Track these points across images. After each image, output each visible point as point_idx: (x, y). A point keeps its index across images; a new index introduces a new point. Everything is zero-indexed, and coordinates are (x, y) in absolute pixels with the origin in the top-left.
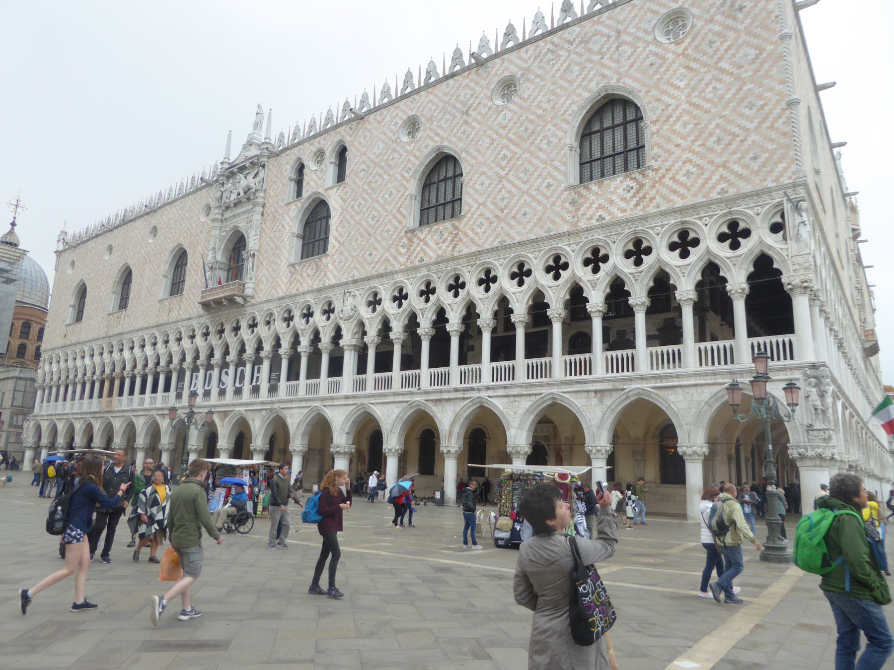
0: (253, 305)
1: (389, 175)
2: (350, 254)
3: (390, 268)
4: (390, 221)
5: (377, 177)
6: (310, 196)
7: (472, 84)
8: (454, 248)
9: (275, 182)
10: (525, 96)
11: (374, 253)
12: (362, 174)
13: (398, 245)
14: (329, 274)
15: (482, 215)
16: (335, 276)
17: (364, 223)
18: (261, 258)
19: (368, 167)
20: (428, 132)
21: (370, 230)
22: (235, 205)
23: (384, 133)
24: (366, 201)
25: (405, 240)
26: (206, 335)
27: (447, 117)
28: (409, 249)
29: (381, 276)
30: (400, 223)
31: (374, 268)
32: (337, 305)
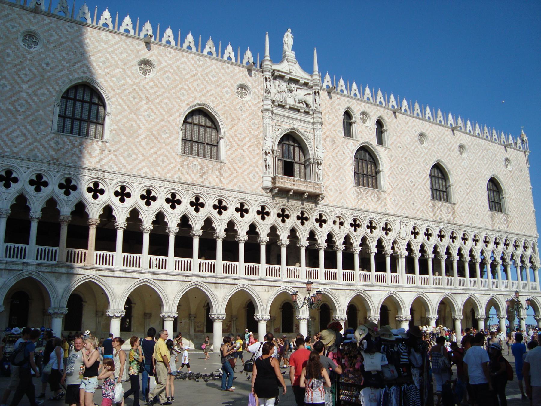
2: (400, 197)
3: (425, 218)
8: (454, 218)
9: (328, 112)
10: (471, 159)
11: (415, 204)
12: (400, 150)
13: (427, 205)
15: (462, 207)
16: (392, 209)
18: (325, 169)
20: (433, 148)
21: (411, 188)
25: (430, 204)
26: (263, 213)
28: (433, 210)
31: (416, 213)
32: (395, 228)
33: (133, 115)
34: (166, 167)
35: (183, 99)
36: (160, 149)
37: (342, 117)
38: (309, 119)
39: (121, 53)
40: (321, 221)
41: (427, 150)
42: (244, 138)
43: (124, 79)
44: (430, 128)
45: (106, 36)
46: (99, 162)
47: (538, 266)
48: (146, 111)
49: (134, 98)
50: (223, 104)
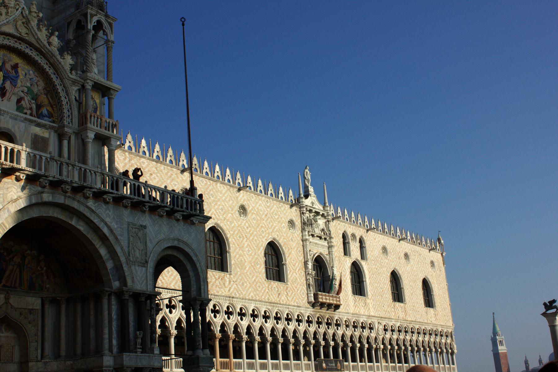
0: (339, 312)
12: (373, 262)
33: (241, 252)
34: (261, 291)
35: (263, 235)
36: (256, 278)
37: (342, 240)
38: (325, 243)
39: (229, 201)
40: (338, 325)
41: (387, 261)
42: (296, 264)
43: (233, 222)
44: (388, 241)
45: (220, 187)
46: (229, 290)
47: (455, 351)
48: (247, 247)
49: (240, 237)
50: (283, 237)
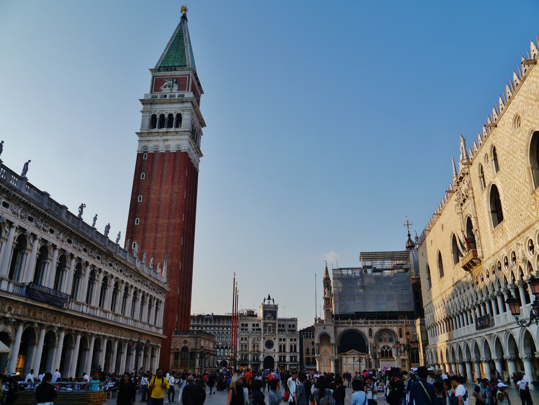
1: (516, 158)
4: (524, 190)
5: (511, 162)
6: (489, 185)
7: (535, 79)
11: (522, 214)
14: (508, 233)
17: (513, 195)
19: (506, 156)
20: (525, 121)
22: (464, 201)
23: (507, 131)
24: (511, 180)
25: (533, 200)
27: (530, 107)
29: (528, 228)
30: (528, 188)
